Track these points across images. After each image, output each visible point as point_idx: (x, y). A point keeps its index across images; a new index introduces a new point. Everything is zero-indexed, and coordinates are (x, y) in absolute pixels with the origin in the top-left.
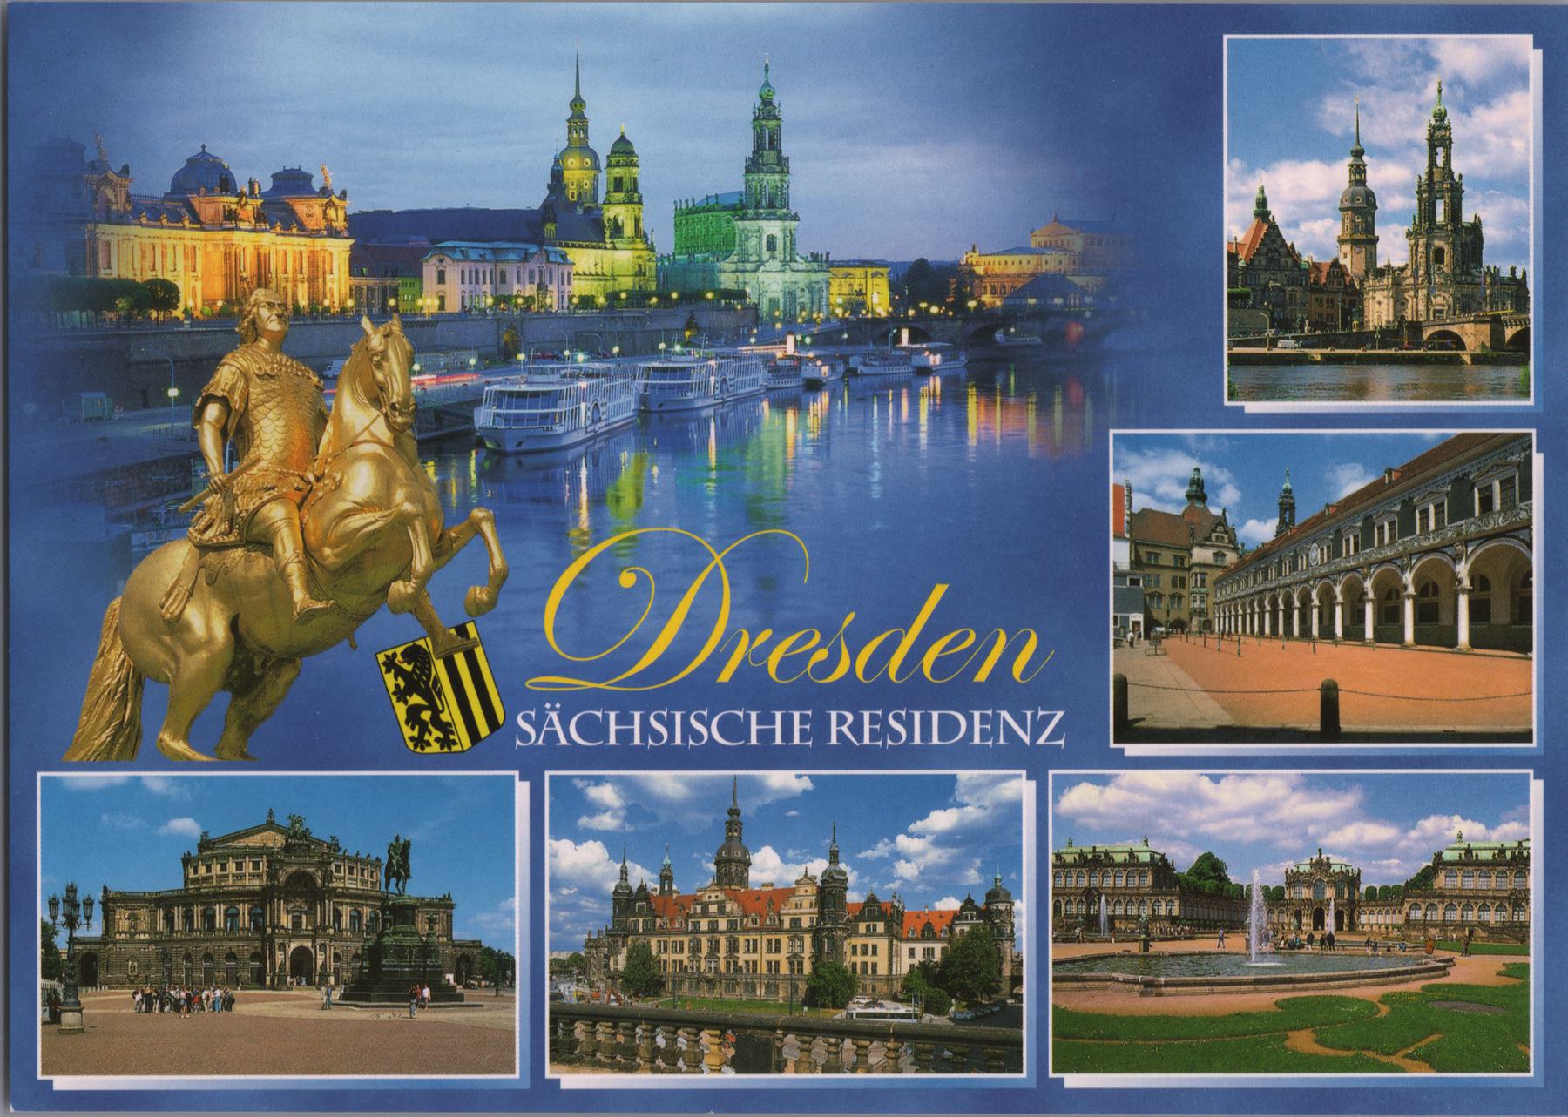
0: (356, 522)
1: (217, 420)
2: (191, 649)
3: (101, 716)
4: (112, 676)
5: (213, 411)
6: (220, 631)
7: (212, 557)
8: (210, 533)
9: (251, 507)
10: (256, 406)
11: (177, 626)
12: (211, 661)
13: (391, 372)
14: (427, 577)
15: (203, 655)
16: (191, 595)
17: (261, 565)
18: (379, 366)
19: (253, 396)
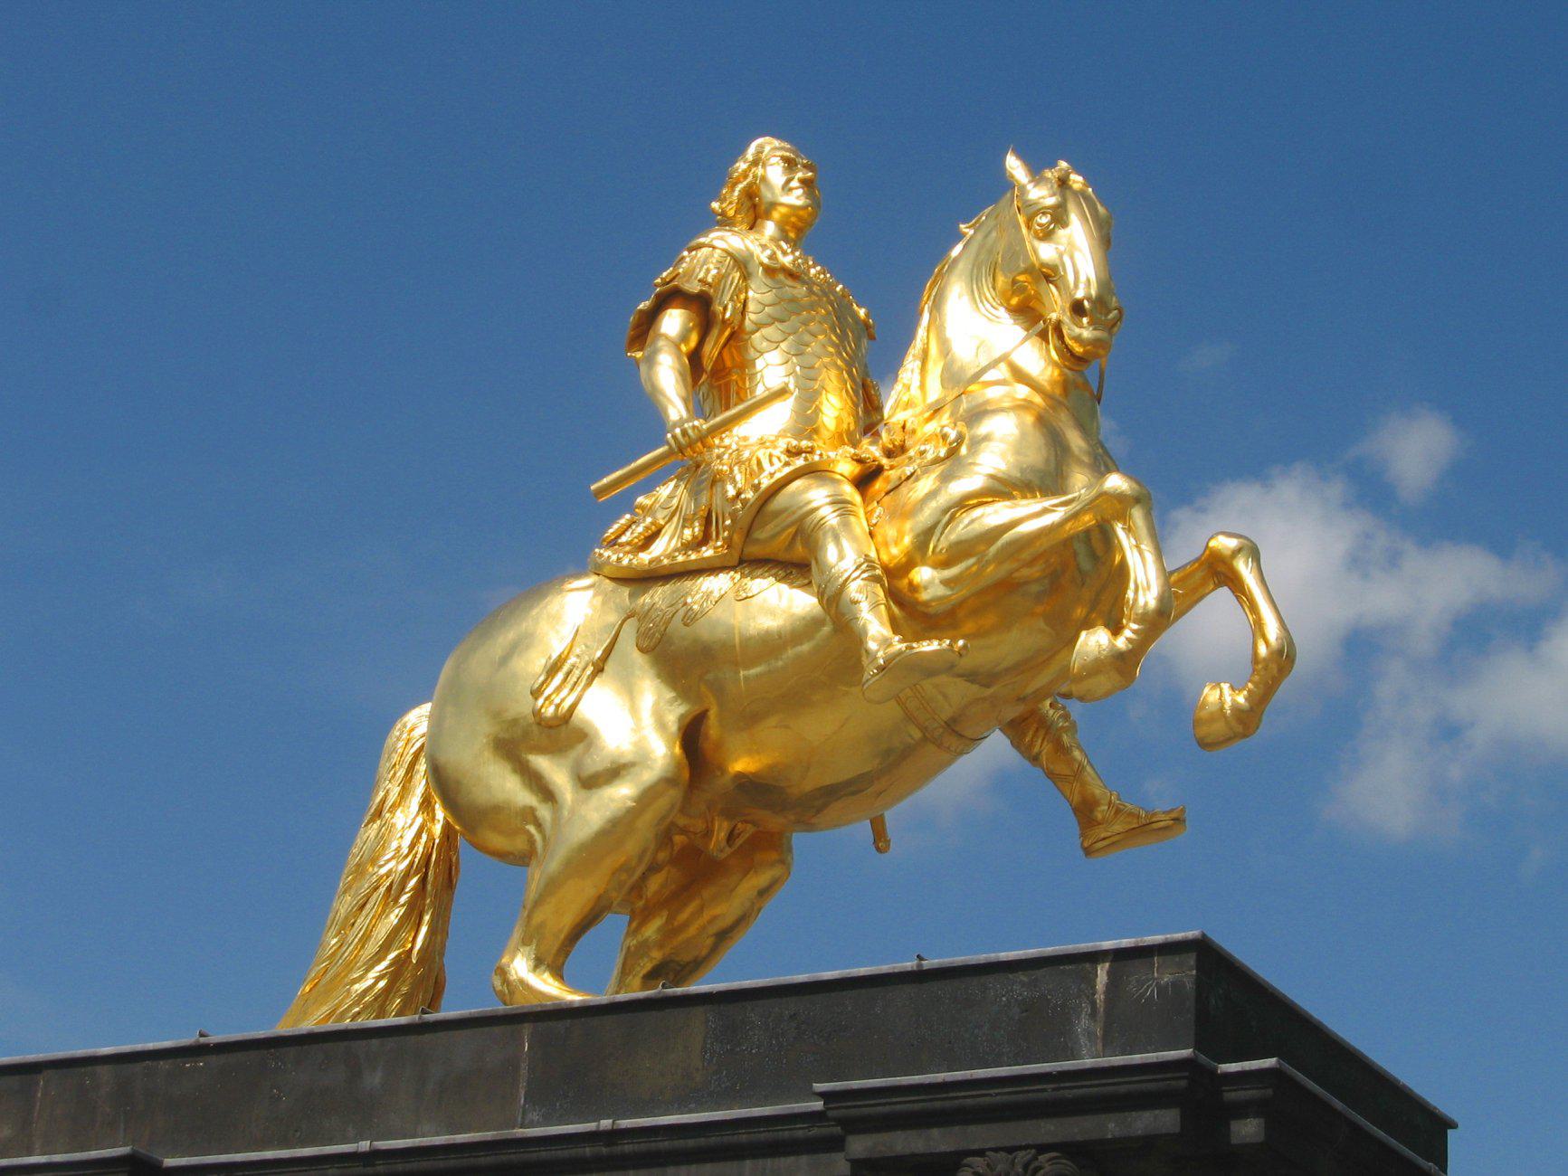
0: (995, 515)
1: (684, 338)
2: (589, 782)
3: (366, 938)
4: (397, 855)
5: (673, 321)
6: (661, 751)
7: (658, 596)
8: (659, 548)
9: (766, 482)
10: (759, 326)
11: (563, 733)
12: (647, 797)
13: (1071, 244)
14: (1159, 621)
15: (622, 793)
16: (599, 669)
17: (775, 604)
18: (1047, 235)
19: (751, 306)
